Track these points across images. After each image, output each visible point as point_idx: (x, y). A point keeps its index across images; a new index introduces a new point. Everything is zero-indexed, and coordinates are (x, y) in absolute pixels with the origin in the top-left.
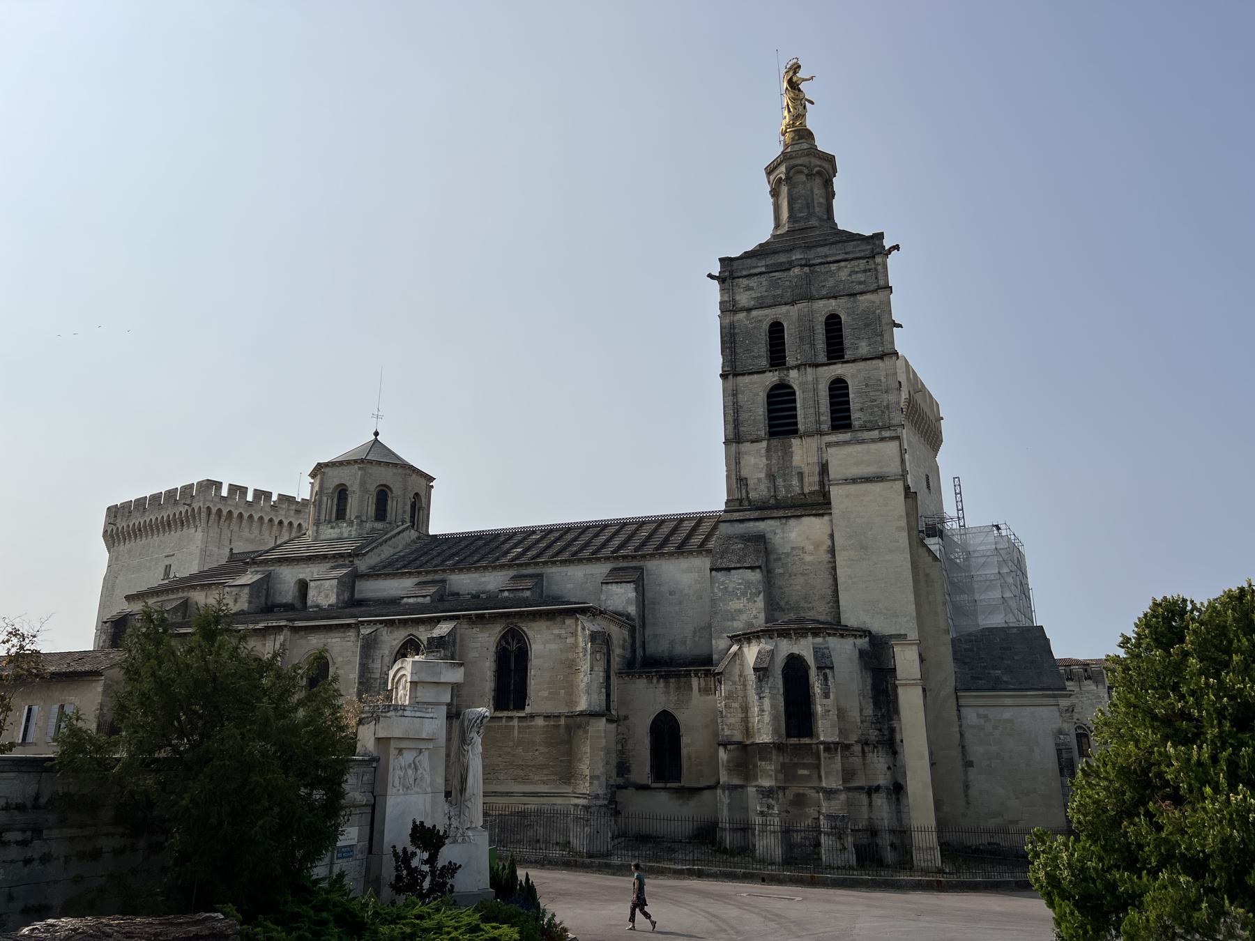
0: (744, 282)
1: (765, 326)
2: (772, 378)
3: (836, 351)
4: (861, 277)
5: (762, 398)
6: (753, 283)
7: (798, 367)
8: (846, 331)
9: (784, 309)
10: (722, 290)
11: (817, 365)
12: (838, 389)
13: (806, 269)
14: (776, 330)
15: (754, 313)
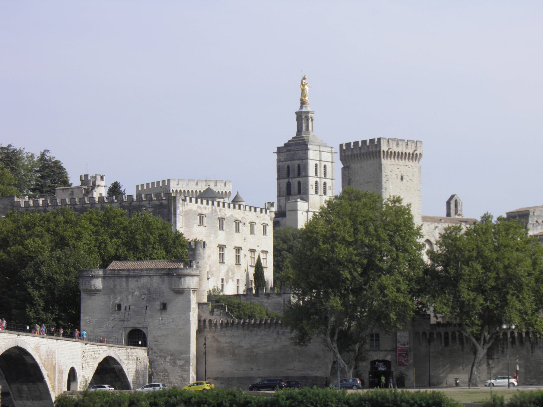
0: (282, 153)
1: (286, 166)
2: (286, 180)
3: (299, 175)
4: (304, 155)
5: (285, 185)
6: (283, 154)
7: (291, 178)
8: (301, 169)
9: (289, 162)
10: (277, 156)
11: (295, 178)
12: (299, 183)
13: (294, 152)
14: (288, 167)
15: (284, 163)
